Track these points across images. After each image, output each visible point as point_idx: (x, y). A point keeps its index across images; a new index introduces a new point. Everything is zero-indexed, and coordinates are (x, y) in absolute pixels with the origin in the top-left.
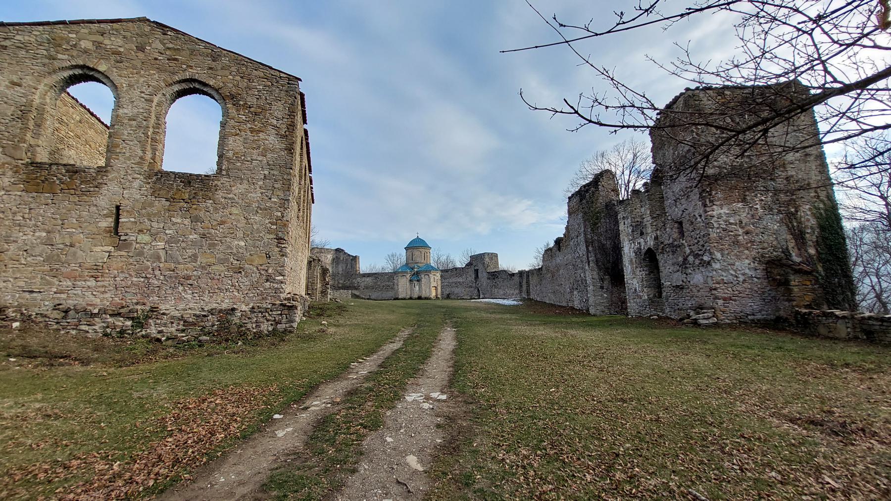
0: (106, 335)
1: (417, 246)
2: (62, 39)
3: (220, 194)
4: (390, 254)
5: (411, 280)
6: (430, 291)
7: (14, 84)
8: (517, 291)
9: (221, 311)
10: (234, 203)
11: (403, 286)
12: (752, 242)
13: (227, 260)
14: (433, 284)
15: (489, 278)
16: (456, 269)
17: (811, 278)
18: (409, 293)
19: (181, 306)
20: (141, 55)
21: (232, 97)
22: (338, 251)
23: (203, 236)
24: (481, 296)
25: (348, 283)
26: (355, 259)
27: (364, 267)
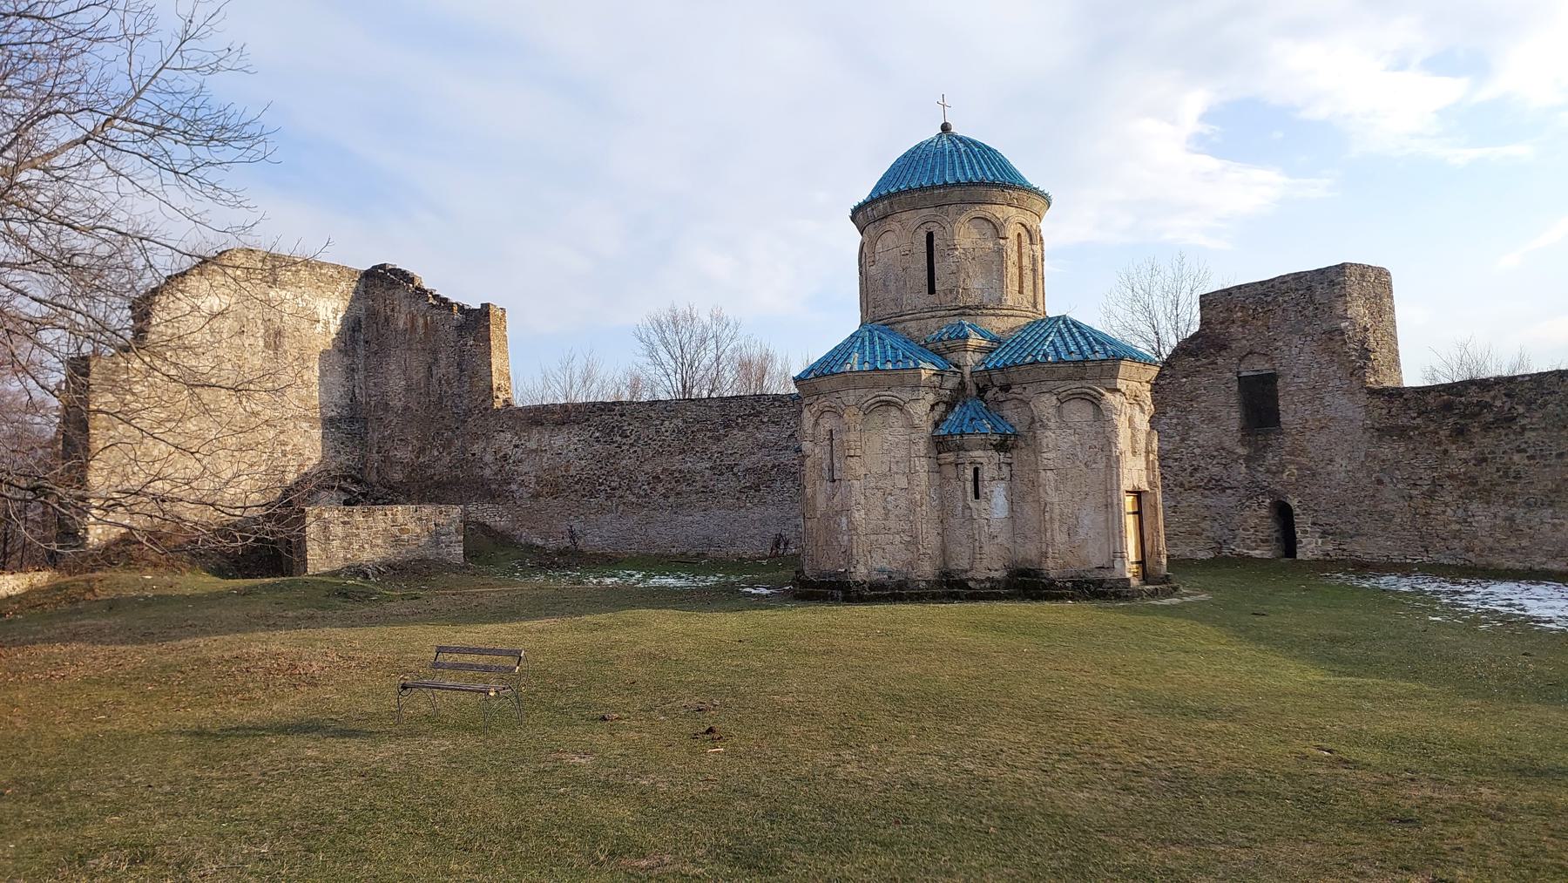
5: (939, 444)
15: (1383, 432)
18: (931, 539)
22: (382, 281)
24: (1310, 546)
25: (442, 463)
26: (478, 323)
27: (526, 371)
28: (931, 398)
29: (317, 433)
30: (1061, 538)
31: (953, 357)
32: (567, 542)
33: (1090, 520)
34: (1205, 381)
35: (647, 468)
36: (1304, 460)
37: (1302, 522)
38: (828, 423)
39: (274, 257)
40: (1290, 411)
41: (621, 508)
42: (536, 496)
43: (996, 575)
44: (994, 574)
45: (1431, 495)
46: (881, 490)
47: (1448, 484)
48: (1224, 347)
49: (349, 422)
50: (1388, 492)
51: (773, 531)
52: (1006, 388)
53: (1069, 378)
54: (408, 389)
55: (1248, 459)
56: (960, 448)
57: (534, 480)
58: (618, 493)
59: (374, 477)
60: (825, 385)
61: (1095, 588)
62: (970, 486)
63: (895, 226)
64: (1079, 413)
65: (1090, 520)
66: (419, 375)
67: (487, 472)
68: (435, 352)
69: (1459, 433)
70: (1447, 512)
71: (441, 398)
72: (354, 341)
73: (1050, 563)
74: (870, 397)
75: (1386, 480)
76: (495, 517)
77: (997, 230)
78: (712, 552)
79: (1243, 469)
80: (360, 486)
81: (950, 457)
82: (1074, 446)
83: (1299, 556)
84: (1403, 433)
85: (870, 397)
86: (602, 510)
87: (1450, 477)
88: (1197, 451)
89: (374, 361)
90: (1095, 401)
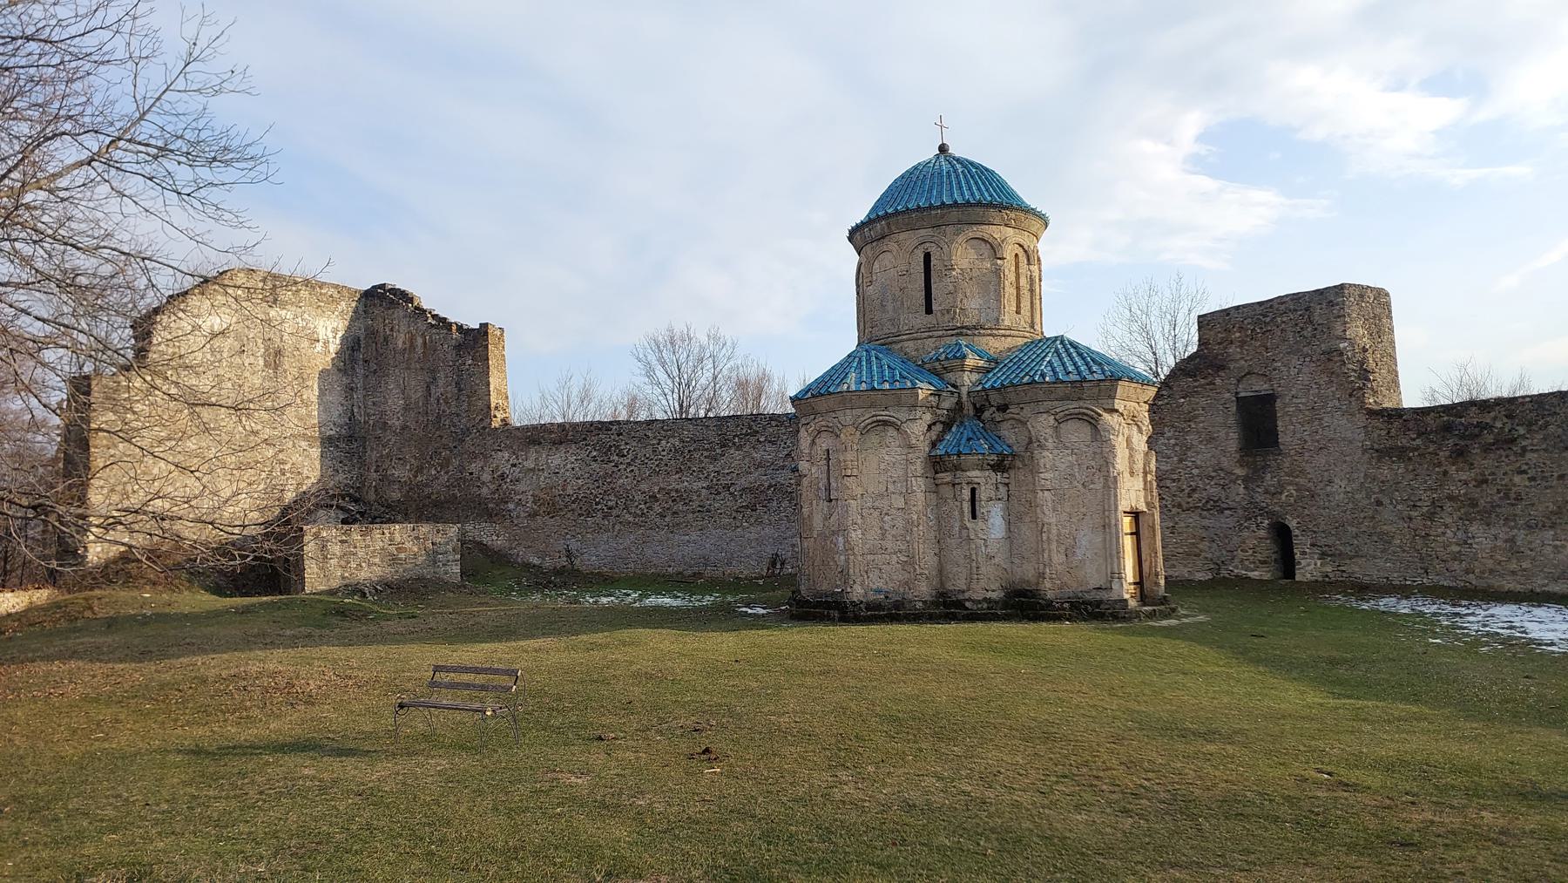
1: (938, 222)
5: (936, 464)
15: (1383, 454)
18: (927, 560)
22: (381, 302)
24: (1309, 568)
25: (439, 481)
26: (475, 343)
28: (928, 417)
29: (315, 452)
30: (1058, 558)
31: (950, 376)
32: (564, 561)
33: (1087, 541)
34: (1203, 402)
35: (644, 486)
36: (1302, 481)
37: (1301, 543)
38: (825, 442)
39: (275, 277)
40: (1290, 431)
41: (617, 527)
42: (533, 515)
43: (994, 595)
44: (989, 595)
45: (1431, 516)
46: (877, 508)
47: (1448, 505)
48: (1222, 367)
49: (347, 441)
50: (1387, 513)
51: (770, 550)
52: (1003, 408)
53: (1066, 398)
54: (407, 408)
55: (1246, 480)
56: (957, 468)
57: (531, 499)
58: (614, 512)
59: (372, 496)
60: (821, 404)
61: (1093, 609)
62: (967, 507)
63: (893, 246)
64: (1077, 433)
65: (1087, 541)
66: (417, 395)
67: (485, 491)
68: (433, 371)
69: (1459, 454)
70: (1447, 534)
71: (439, 417)
72: (353, 360)
73: (1048, 584)
74: (867, 416)
75: (1386, 501)
76: (491, 535)
77: (995, 250)
78: (708, 572)
79: (1241, 490)
80: (357, 504)
81: (946, 477)
82: (1071, 466)
83: (1298, 578)
84: (1401, 454)
85: (867, 416)
86: (599, 528)
87: (1451, 498)
88: (1195, 472)
89: (373, 380)
90: (1093, 422)
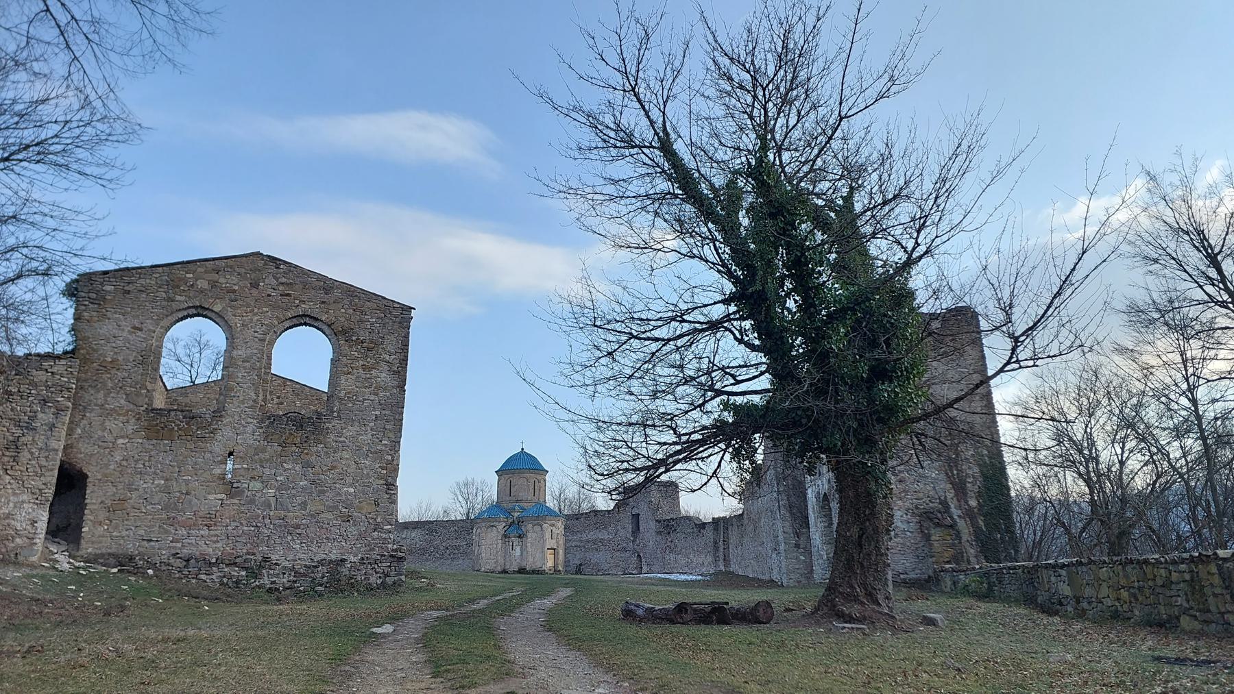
0: (222, 584)
2: (180, 279)
3: (331, 437)
4: (461, 479)
5: (505, 536)
6: (544, 558)
7: (135, 328)
8: (710, 559)
9: (331, 562)
10: (345, 447)
11: (490, 548)
12: (906, 492)
13: (336, 508)
14: (551, 543)
16: (596, 512)
17: (952, 532)
19: (291, 557)
20: (255, 292)
21: (345, 332)
23: (313, 482)
24: (645, 569)
64: (537, 528)
